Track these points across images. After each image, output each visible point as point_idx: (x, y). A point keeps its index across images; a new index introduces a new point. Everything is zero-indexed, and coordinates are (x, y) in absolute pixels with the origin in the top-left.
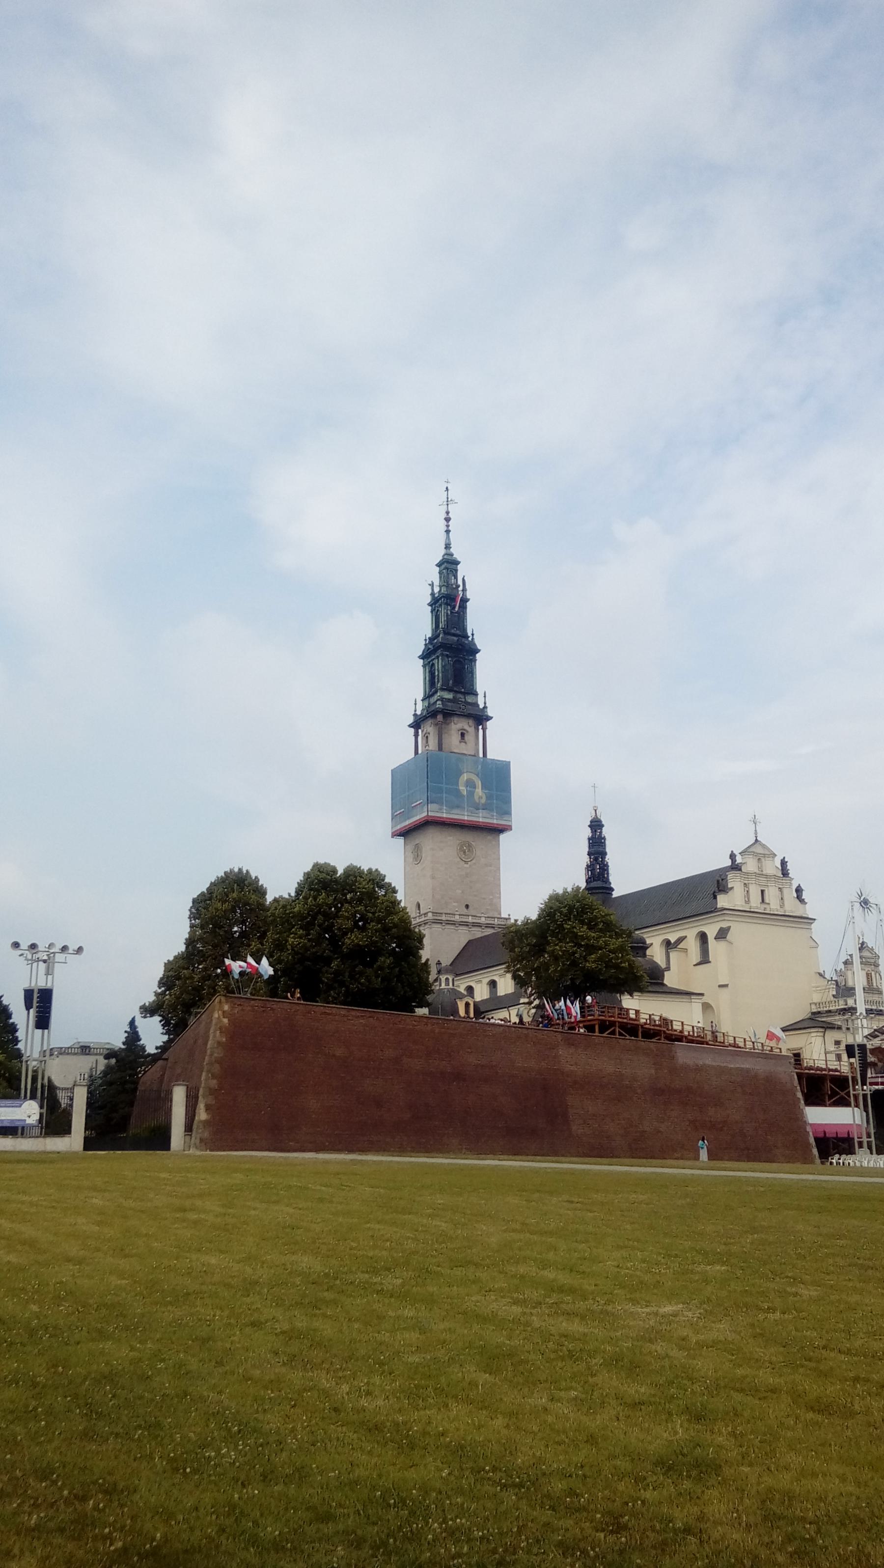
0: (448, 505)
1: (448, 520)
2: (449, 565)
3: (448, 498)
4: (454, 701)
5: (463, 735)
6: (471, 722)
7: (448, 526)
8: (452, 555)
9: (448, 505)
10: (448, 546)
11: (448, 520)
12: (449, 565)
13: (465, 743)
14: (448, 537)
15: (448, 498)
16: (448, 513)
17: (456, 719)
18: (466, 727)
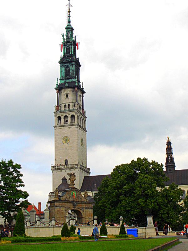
0: (69, 6)
1: (69, 12)
2: (70, 29)
3: (69, 4)
4: (65, 82)
5: (67, 96)
6: (70, 89)
7: (69, 14)
8: (70, 25)
9: (69, 6)
10: (69, 22)
11: (69, 12)
12: (70, 29)
13: (68, 98)
14: (69, 19)
15: (69, 4)
16: (69, 9)
17: (63, 90)
18: (68, 92)
